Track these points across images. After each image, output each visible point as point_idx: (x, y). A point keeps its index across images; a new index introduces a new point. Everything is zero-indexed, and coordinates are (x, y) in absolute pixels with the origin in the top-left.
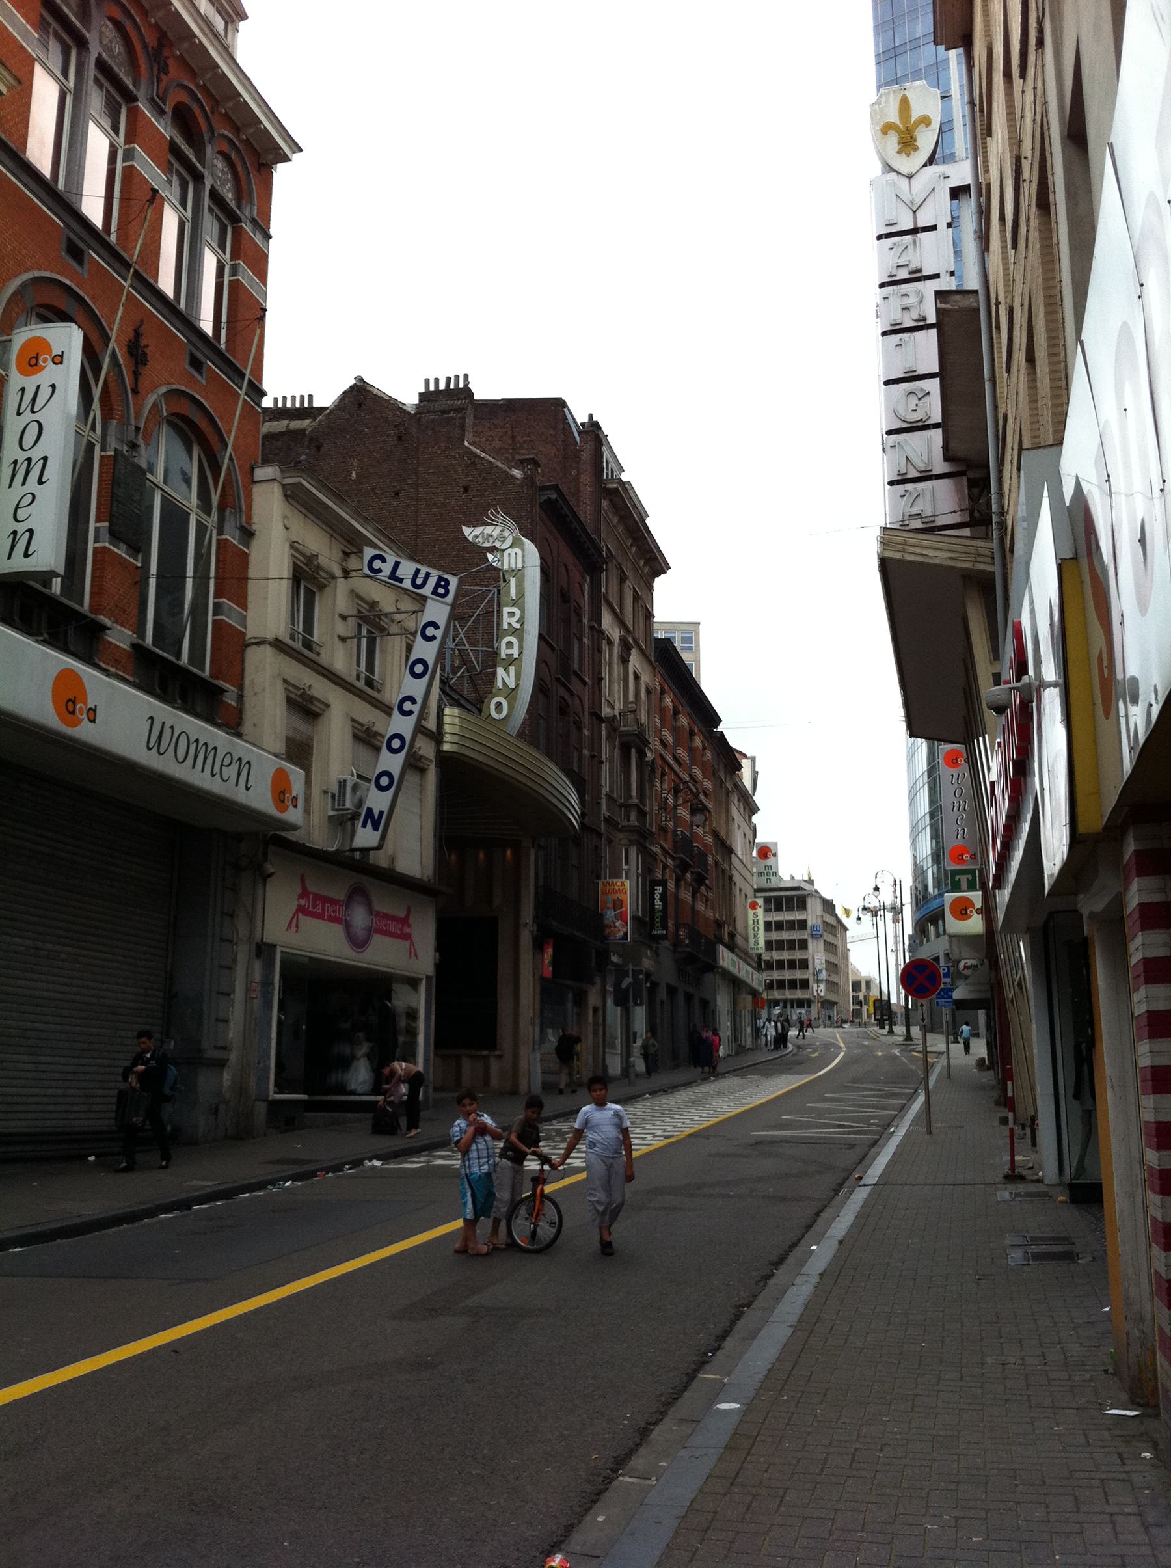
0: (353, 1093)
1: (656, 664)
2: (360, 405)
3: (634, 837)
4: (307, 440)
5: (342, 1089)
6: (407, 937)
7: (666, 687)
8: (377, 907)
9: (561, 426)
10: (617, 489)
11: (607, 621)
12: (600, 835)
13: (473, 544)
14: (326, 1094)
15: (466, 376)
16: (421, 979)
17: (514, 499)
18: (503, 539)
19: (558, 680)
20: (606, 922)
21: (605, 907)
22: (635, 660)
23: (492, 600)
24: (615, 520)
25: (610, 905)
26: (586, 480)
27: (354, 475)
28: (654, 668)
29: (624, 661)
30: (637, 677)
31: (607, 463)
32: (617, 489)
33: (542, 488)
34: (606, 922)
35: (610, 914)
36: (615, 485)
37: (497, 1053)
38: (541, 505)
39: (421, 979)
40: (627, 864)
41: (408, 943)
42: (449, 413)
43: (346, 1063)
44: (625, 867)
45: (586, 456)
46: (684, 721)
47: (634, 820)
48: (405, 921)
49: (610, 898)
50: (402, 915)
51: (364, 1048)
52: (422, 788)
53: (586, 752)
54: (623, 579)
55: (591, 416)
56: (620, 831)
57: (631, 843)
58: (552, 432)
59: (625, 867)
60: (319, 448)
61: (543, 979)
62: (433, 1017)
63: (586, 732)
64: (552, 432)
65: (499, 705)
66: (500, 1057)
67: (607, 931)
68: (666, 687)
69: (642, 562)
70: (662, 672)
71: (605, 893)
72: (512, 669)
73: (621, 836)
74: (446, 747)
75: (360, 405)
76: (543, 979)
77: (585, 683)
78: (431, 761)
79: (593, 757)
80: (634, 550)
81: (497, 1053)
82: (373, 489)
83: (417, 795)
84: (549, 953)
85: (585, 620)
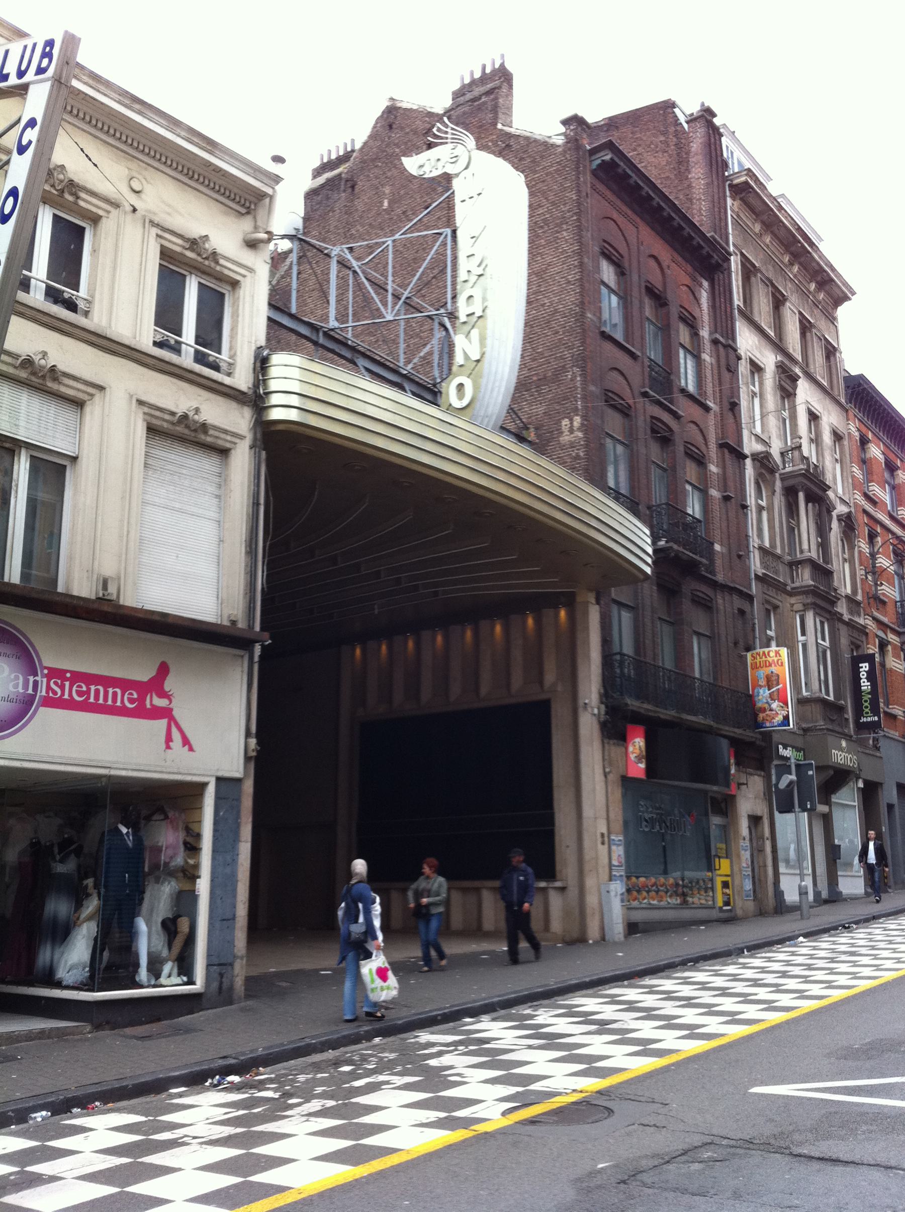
0: (59, 985)
1: (848, 406)
2: (390, 126)
3: (810, 600)
4: (343, 183)
5: (50, 979)
6: (166, 713)
7: (870, 436)
8: (49, 659)
9: (672, 129)
10: (746, 183)
11: (747, 341)
12: (750, 598)
13: (421, 178)
14: (31, 984)
15: (503, 56)
16: (204, 785)
17: (557, 171)
18: (455, 159)
19: (645, 395)
20: (759, 705)
21: (756, 685)
22: (805, 392)
23: (444, 244)
24: (757, 228)
25: (762, 682)
26: (698, 174)
27: (386, 204)
28: (847, 411)
29: (787, 392)
30: (813, 417)
31: (727, 147)
32: (746, 183)
33: (593, 152)
34: (759, 705)
35: (763, 694)
36: (743, 179)
37: (558, 884)
38: (594, 173)
39: (204, 785)
40: (804, 633)
41: (164, 722)
42: (480, 99)
43: (62, 933)
44: (801, 638)
45: (697, 145)
46: (875, 451)
47: (806, 578)
48: (156, 685)
49: (762, 673)
50: (144, 674)
51: (92, 905)
52: (223, 480)
53: (714, 493)
54: (778, 302)
55: (703, 104)
56: (791, 594)
57: (806, 607)
58: (662, 138)
59: (801, 638)
60: (353, 187)
61: (626, 781)
62: (245, 849)
63: (713, 468)
64: (662, 138)
65: (461, 386)
66: (563, 889)
67: (761, 715)
68: (870, 436)
69: (813, 286)
70: (860, 415)
71: (755, 667)
72: (475, 333)
73: (793, 600)
74: (276, 414)
75: (390, 126)
76: (626, 781)
77: (707, 409)
78: (242, 437)
79: (727, 498)
80: (796, 268)
81: (558, 884)
82: (404, 213)
83: (212, 489)
84: (637, 745)
85: (705, 333)
